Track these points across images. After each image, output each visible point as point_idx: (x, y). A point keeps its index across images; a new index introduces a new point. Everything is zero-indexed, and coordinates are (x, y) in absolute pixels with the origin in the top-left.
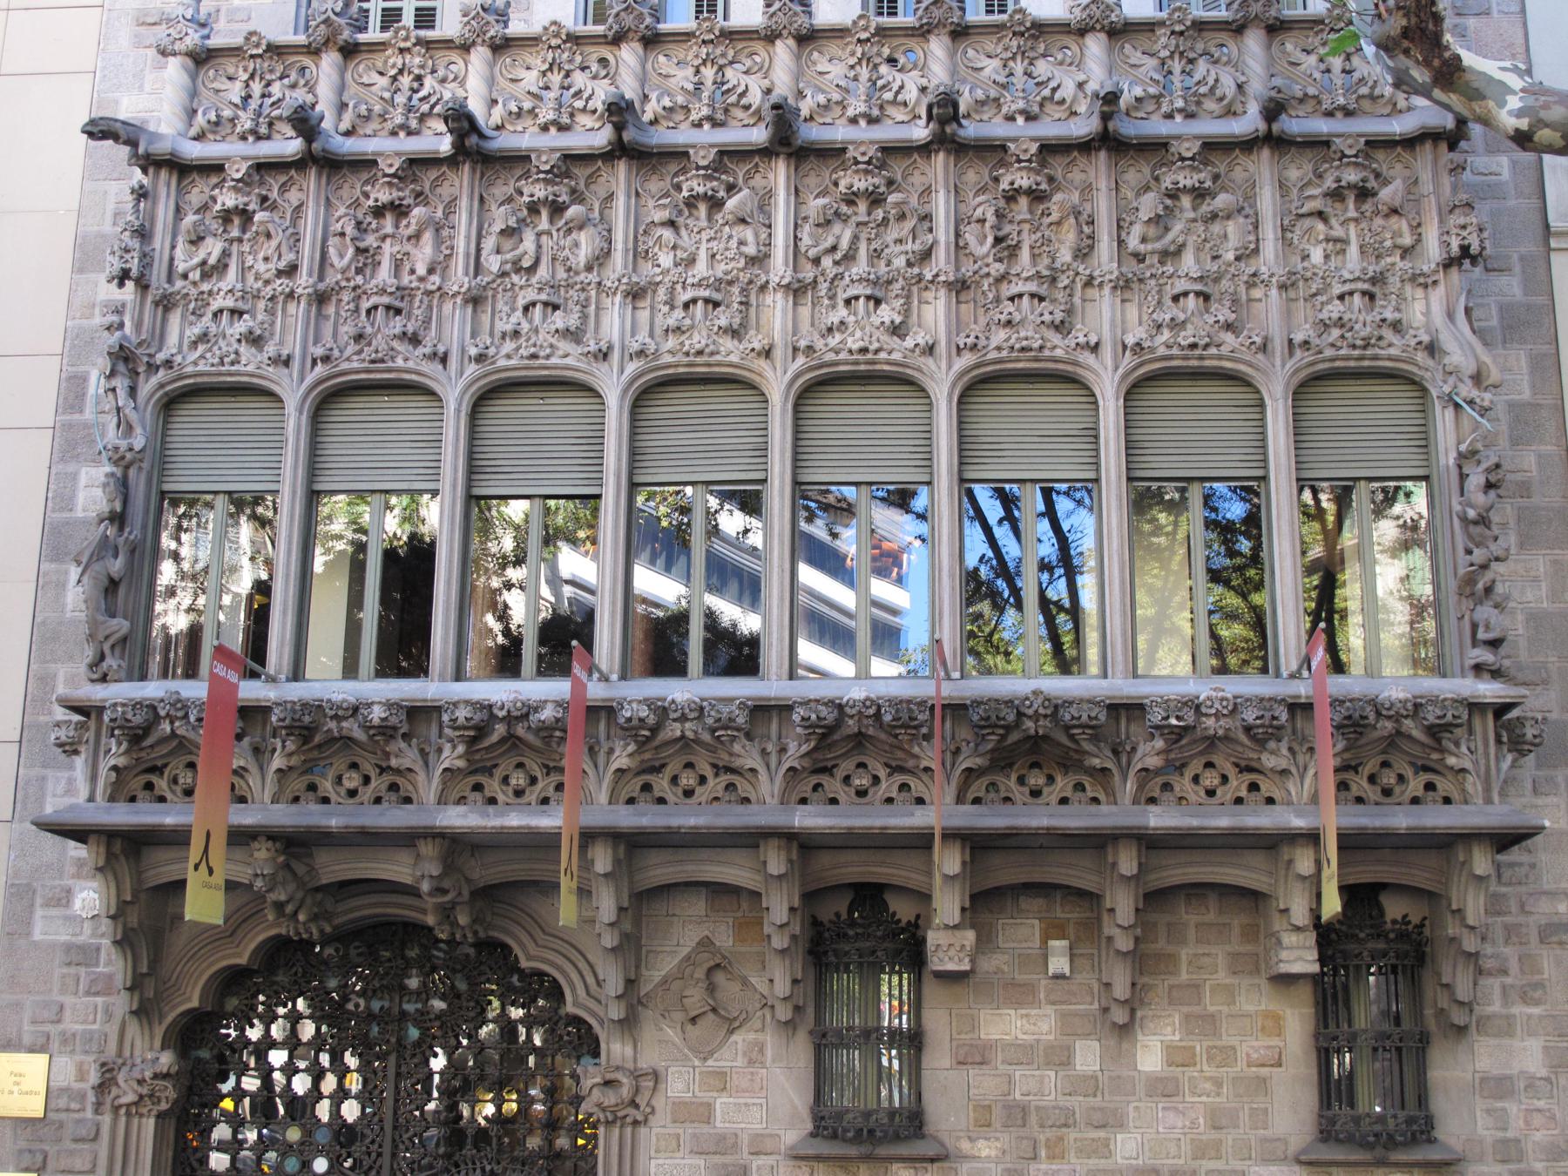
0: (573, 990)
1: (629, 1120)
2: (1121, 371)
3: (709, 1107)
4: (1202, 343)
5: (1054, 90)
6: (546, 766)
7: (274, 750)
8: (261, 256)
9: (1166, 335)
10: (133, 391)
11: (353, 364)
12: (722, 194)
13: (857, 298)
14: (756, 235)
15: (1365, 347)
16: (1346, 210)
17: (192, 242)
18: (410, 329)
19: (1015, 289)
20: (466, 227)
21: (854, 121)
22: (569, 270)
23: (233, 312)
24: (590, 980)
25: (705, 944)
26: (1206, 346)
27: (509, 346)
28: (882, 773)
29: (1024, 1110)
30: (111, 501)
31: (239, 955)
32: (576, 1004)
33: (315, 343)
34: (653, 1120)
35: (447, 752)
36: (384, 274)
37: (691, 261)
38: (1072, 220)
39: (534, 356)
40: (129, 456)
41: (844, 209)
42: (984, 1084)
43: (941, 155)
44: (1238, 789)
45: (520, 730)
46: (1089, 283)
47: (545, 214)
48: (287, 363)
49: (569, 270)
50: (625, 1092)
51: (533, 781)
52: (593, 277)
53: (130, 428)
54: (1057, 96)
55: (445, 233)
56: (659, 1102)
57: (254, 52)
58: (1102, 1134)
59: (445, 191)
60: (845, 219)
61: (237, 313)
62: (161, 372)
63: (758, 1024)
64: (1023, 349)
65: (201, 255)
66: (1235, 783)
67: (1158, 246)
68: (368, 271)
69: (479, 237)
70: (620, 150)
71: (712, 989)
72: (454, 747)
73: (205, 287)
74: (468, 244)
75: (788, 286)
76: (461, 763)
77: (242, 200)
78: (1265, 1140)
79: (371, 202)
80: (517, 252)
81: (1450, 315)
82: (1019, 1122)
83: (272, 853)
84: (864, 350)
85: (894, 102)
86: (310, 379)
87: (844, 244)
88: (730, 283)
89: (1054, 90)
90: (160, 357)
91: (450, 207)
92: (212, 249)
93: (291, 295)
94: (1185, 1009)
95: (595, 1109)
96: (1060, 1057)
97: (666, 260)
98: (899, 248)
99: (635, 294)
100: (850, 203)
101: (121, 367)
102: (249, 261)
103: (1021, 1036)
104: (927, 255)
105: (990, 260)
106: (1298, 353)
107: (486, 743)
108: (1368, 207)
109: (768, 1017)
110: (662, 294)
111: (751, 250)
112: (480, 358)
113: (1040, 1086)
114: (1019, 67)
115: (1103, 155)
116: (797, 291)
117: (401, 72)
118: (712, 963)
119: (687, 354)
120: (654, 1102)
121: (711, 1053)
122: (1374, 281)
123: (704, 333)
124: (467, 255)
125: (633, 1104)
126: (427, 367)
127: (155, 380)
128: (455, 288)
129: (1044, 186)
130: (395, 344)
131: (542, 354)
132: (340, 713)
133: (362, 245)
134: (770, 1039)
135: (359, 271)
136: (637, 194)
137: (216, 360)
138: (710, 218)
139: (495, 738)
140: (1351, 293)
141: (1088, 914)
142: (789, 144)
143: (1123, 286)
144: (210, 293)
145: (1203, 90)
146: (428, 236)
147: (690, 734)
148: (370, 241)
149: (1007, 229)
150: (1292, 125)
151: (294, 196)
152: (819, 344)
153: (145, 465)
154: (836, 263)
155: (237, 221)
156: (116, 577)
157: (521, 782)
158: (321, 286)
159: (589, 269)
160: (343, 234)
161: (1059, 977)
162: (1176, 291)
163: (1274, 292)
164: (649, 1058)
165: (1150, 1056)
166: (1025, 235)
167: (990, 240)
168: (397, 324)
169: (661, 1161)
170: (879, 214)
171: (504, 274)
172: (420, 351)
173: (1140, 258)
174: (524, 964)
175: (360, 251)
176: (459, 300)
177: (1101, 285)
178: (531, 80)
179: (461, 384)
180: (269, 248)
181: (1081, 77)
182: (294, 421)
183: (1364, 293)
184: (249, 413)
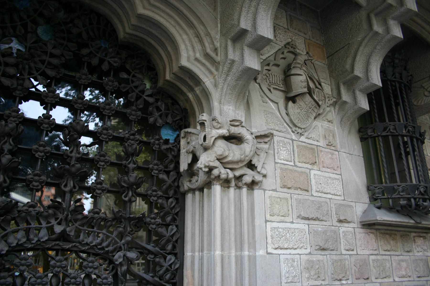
34: (268, 183)
50: (247, 148)
95: (217, 164)
169: (275, 225)
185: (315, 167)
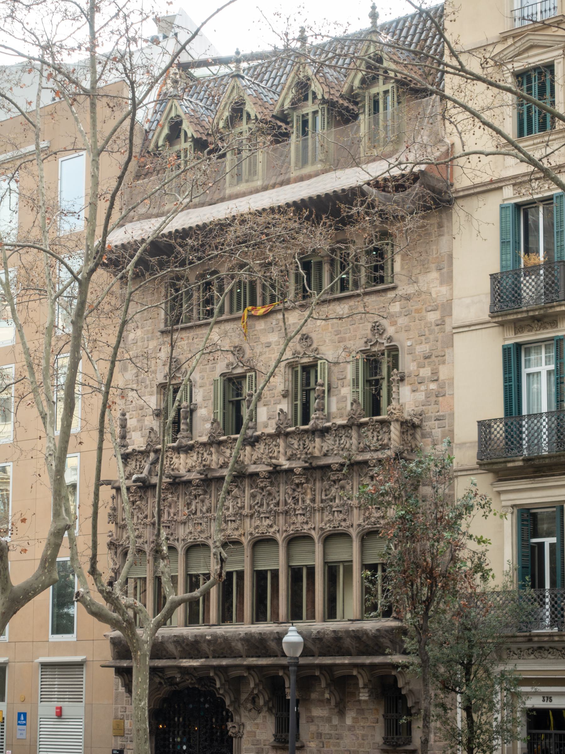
3: (255, 732)
29: (321, 734)
34: (244, 736)
42: (313, 728)
50: (237, 729)
56: (245, 732)
78: (374, 743)
96: (329, 720)
111: (239, 505)
113: (326, 729)
125: (239, 732)
134: (267, 715)
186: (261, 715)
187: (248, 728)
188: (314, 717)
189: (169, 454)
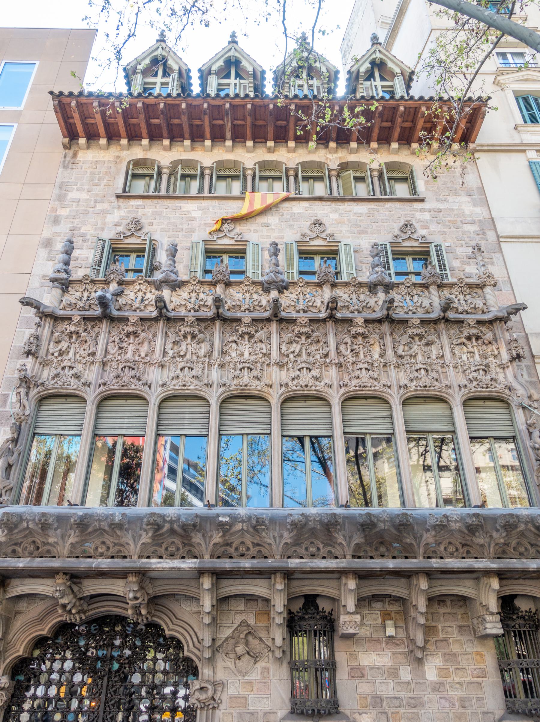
0: (188, 644)
1: (211, 706)
2: (400, 395)
3: (246, 698)
4: (428, 385)
5: (367, 303)
6: (184, 543)
7: (70, 535)
8: (82, 348)
9: (415, 383)
10: (27, 394)
11: (114, 387)
12: (253, 333)
13: (303, 368)
14: (266, 347)
15: (487, 388)
16: (472, 343)
17: (56, 342)
18: (138, 375)
19: (359, 367)
20: (159, 341)
21: (298, 312)
22: (198, 357)
23: (70, 367)
24: (195, 640)
25: (244, 623)
26: (430, 387)
27: (175, 382)
28: (321, 546)
30: (13, 433)
31: (43, 630)
32: (189, 651)
33: (101, 378)
34: (222, 707)
35: (144, 536)
36: (129, 355)
37: (241, 355)
38: (378, 343)
39: (184, 385)
40: (23, 417)
41: (297, 339)
43: (330, 322)
44: (463, 553)
45: (175, 526)
46: (385, 366)
47: (189, 337)
48: (89, 386)
49: (198, 357)
50: (210, 693)
51: (178, 549)
52: (207, 359)
53: (24, 407)
54: (368, 305)
55: (152, 343)
56: (224, 698)
57: (86, 282)
58: (414, 710)
59: (153, 330)
60: (297, 342)
61: (71, 368)
62: (39, 387)
63: (267, 659)
64: (364, 386)
65: (60, 347)
66: (461, 551)
67: (409, 353)
68: (123, 355)
69: (165, 345)
70: (218, 316)
71: (247, 644)
72: (147, 534)
73: (60, 358)
74: (161, 346)
75: (278, 363)
76: (149, 541)
77: (77, 329)
79: (125, 332)
80: (180, 349)
81: (515, 377)
82: (380, 705)
83: (65, 581)
84: (306, 386)
85: (312, 306)
86: (98, 391)
87: (297, 350)
88: (256, 362)
89: (367, 303)
90: (41, 381)
91: (155, 335)
92: (64, 345)
93: (92, 363)
94: (443, 651)
95: (196, 701)
96: (394, 673)
97: (234, 354)
98: (316, 352)
99: (222, 366)
100: (299, 337)
101: (24, 384)
102: (78, 350)
103: (377, 664)
104: (326, 355)
105: (350, 356)
106: (463, 390)
107: (161, 532)
108: (480, 342)
109: (271, 656)
110: (232, 365)
111: (264, 351)
112: (163, 385)
114: (354, 296)
115: (386, 323)
116: (281, 365)
117: (139, 291)
118: (247, 631)
119: (241, 386)
120: (222, 698)
121: (247, 673)
122: (486, 366)
123: (248, 379)
124: (161, 351)
125: (213, 699)
126: (142, 388)
127: (36, 390)
128: (156, 361)
129: (367, 333)
130: (132, 380)
131: (187, 384)
132: (101, 518)
133: (121, 346)
134: (272, 666)
135: (119, 355)
136: (223, 333)
137: (62, 384)
138: (249, 341)
139: (165, 529)
140: (478, 370)
141: (399, 609)
142: (277, 317)
143: (397, 366)
144: (62, 360)
145: (418, 305)
146: (146, 344)
147: (245, 528)
148: (124, 345)
149: (355, 347)
150: (451, 315)
151: (96, 330)
152: (290, 384)
153: (29, 422)
154: (295, 357)
155: (74, 337)
156: (11, 463)
157: (174, 549)
158: (105, 360)
159: (205, 357)
160: (114, 342)
161: (391, 637)
162: (416, 368)
163: (451, 368)
164: (221, 675)
165: (431, 671)
166: (361, 349)
167: (349, 350)
168: (133, 373)
170: (309, 341)
171: (174, 357)
172: (141, 383)
173: (401, 357)
174: (167, 633)
175: (120, 348)
176: (157, 365)
177: (390, 365)
178: (185, 295)
179: (156, 394)
180: (86, 346)
181: (376, 299)
182: (90, 408)
183: (483, 370)
184: (72, 406)
185: (252, 693)
186: (258, 665)
187: (232, 690)
188: (364, 668)
189: (143, 288)
